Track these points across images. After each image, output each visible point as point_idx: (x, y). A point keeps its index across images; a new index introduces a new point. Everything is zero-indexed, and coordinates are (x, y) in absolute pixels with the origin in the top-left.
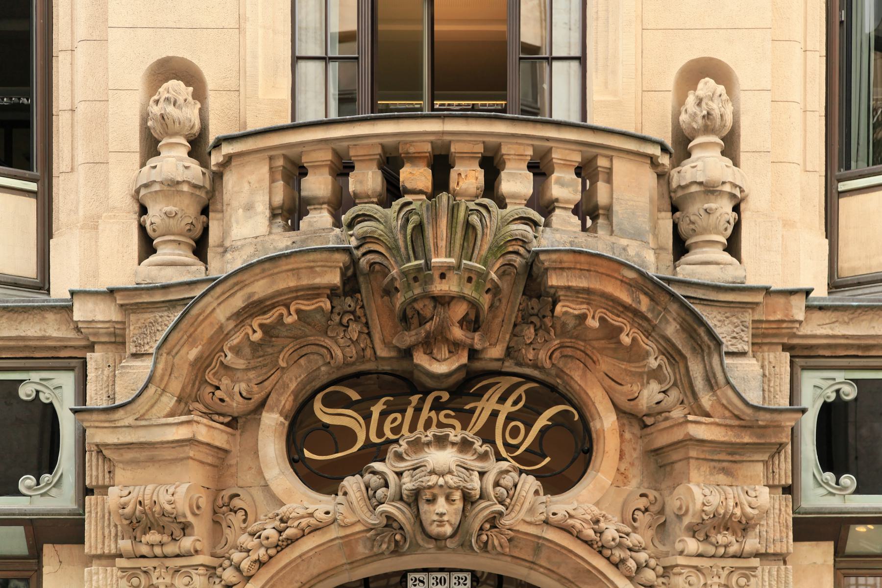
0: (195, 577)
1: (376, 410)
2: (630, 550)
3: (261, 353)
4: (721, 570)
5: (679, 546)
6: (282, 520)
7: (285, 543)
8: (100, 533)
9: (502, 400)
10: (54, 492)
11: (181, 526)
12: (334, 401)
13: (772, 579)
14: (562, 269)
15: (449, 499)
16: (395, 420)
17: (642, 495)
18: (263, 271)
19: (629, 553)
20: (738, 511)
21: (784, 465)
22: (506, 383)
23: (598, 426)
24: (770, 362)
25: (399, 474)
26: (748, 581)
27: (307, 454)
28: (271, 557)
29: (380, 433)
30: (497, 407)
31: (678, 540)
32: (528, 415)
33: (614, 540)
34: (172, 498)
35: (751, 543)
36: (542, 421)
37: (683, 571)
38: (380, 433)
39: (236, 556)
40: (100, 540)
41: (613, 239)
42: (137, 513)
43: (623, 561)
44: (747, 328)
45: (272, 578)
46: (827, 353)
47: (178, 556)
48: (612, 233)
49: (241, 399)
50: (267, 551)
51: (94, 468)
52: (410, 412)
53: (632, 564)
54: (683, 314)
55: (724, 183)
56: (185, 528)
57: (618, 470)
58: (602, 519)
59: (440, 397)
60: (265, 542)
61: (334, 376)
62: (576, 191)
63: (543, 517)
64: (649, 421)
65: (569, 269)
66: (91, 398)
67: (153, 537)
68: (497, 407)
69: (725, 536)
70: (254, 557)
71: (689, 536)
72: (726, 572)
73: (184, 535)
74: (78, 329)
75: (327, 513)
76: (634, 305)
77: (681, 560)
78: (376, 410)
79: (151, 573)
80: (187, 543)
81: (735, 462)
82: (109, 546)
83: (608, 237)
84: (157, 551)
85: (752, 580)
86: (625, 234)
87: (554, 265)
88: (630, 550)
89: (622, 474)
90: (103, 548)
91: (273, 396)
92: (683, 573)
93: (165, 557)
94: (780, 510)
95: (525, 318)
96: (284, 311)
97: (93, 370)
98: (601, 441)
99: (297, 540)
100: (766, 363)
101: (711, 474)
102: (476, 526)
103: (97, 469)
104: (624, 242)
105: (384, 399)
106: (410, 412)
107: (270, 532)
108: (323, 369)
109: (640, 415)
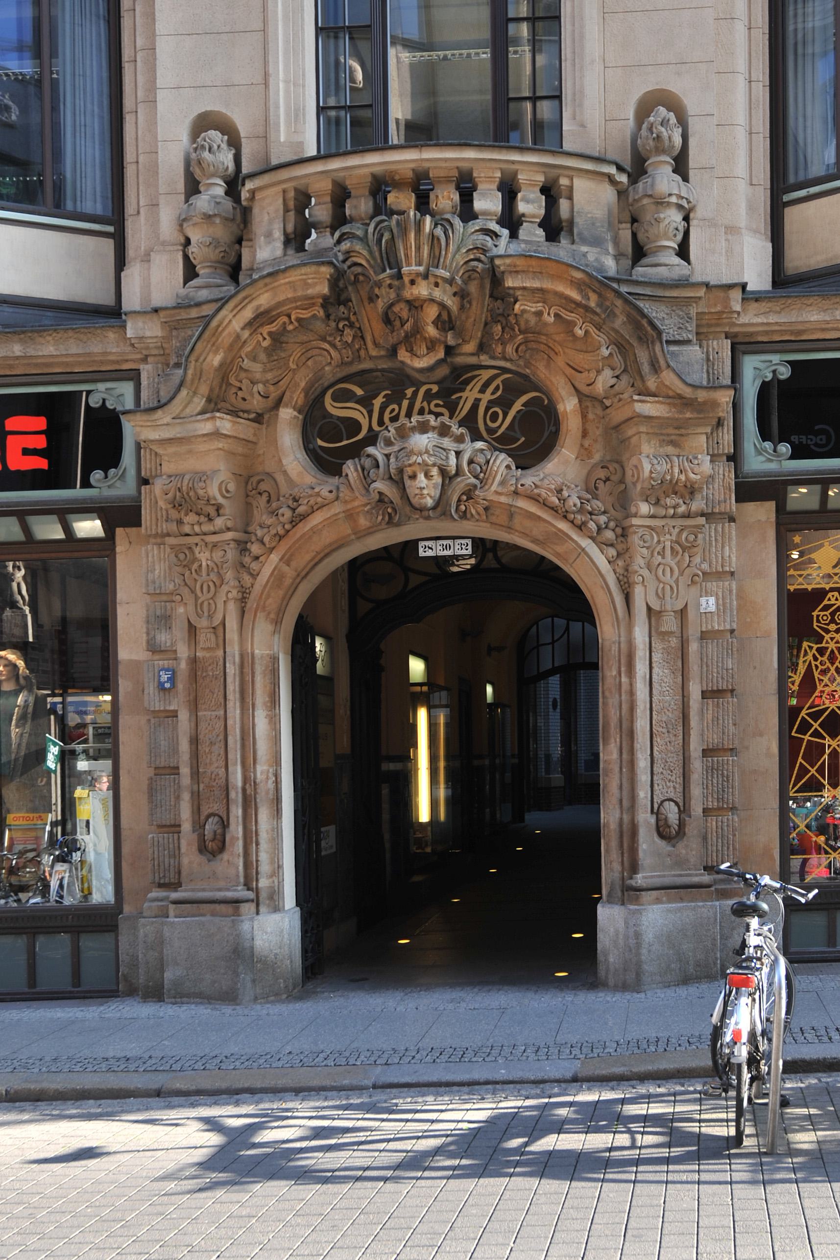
0: (229, 552)
1: (378, 402)
2: (591, 514)
3: (276, 358)
4: (671, 529)
7: (298, 519)
9: (482, 391)
10: (118, 484)
11: (215, 507)
12: (343, 396)
14: (517, 272)
15: (427, 476)
16: (393, 410)
18: (266, 285)
20: (683, 477)
21: (727, 436)
22: (486, 375)
24: (713, 349)
25: (388, 456)
27: (320, 442)
28: (288, 531)
29: (381, 423)
30: (479, 396)
33: (575, 505)
35: (697, 505)
36: (518, 406)
38: (381, 423)
40: (154, 522)
41: (574, 247)
43: (584, 523)
44: (690, 318)
45: (290, 548)
46: (765, 339)
47: (214, 533)
48: (573, 243)
51: (148, 462)
52: (405, 403)
53: (592, 525)
54: (628, 309)
55: (670, 195)
57: (582, 445)
58: (565, 488)
59: (431, 390)
60: (281, 519)
61: (339, 375)
62: (540, 207)
63: (513, 489)
64: (607, 403)
65: (523, 271)
66: (144, 403)
68: (479, 396)
72: (677, 530)
73: (219, 515)
74: (133, 345)
76: (583, 302)
78: (378, 402)
81: (682, 435)
82: (162, 526)
83: (569, 246)
84: (197, 529)
85: (700, 536)
86: (584, 241)
87: (509, 269)
88: (591, 514)
89: (586, 449)
91: (288, 394)
93: (205, 534)
95: (495, 317)
96: (285, 319)
98: (565, 422)
100: (711, 349)
101: (661, 446)
102: (455, 498)
103: (151, 462)
104: (584, 249)
105: (383, 394)
106: (405, 403)
108: (327, 368)
109: (600, 398)
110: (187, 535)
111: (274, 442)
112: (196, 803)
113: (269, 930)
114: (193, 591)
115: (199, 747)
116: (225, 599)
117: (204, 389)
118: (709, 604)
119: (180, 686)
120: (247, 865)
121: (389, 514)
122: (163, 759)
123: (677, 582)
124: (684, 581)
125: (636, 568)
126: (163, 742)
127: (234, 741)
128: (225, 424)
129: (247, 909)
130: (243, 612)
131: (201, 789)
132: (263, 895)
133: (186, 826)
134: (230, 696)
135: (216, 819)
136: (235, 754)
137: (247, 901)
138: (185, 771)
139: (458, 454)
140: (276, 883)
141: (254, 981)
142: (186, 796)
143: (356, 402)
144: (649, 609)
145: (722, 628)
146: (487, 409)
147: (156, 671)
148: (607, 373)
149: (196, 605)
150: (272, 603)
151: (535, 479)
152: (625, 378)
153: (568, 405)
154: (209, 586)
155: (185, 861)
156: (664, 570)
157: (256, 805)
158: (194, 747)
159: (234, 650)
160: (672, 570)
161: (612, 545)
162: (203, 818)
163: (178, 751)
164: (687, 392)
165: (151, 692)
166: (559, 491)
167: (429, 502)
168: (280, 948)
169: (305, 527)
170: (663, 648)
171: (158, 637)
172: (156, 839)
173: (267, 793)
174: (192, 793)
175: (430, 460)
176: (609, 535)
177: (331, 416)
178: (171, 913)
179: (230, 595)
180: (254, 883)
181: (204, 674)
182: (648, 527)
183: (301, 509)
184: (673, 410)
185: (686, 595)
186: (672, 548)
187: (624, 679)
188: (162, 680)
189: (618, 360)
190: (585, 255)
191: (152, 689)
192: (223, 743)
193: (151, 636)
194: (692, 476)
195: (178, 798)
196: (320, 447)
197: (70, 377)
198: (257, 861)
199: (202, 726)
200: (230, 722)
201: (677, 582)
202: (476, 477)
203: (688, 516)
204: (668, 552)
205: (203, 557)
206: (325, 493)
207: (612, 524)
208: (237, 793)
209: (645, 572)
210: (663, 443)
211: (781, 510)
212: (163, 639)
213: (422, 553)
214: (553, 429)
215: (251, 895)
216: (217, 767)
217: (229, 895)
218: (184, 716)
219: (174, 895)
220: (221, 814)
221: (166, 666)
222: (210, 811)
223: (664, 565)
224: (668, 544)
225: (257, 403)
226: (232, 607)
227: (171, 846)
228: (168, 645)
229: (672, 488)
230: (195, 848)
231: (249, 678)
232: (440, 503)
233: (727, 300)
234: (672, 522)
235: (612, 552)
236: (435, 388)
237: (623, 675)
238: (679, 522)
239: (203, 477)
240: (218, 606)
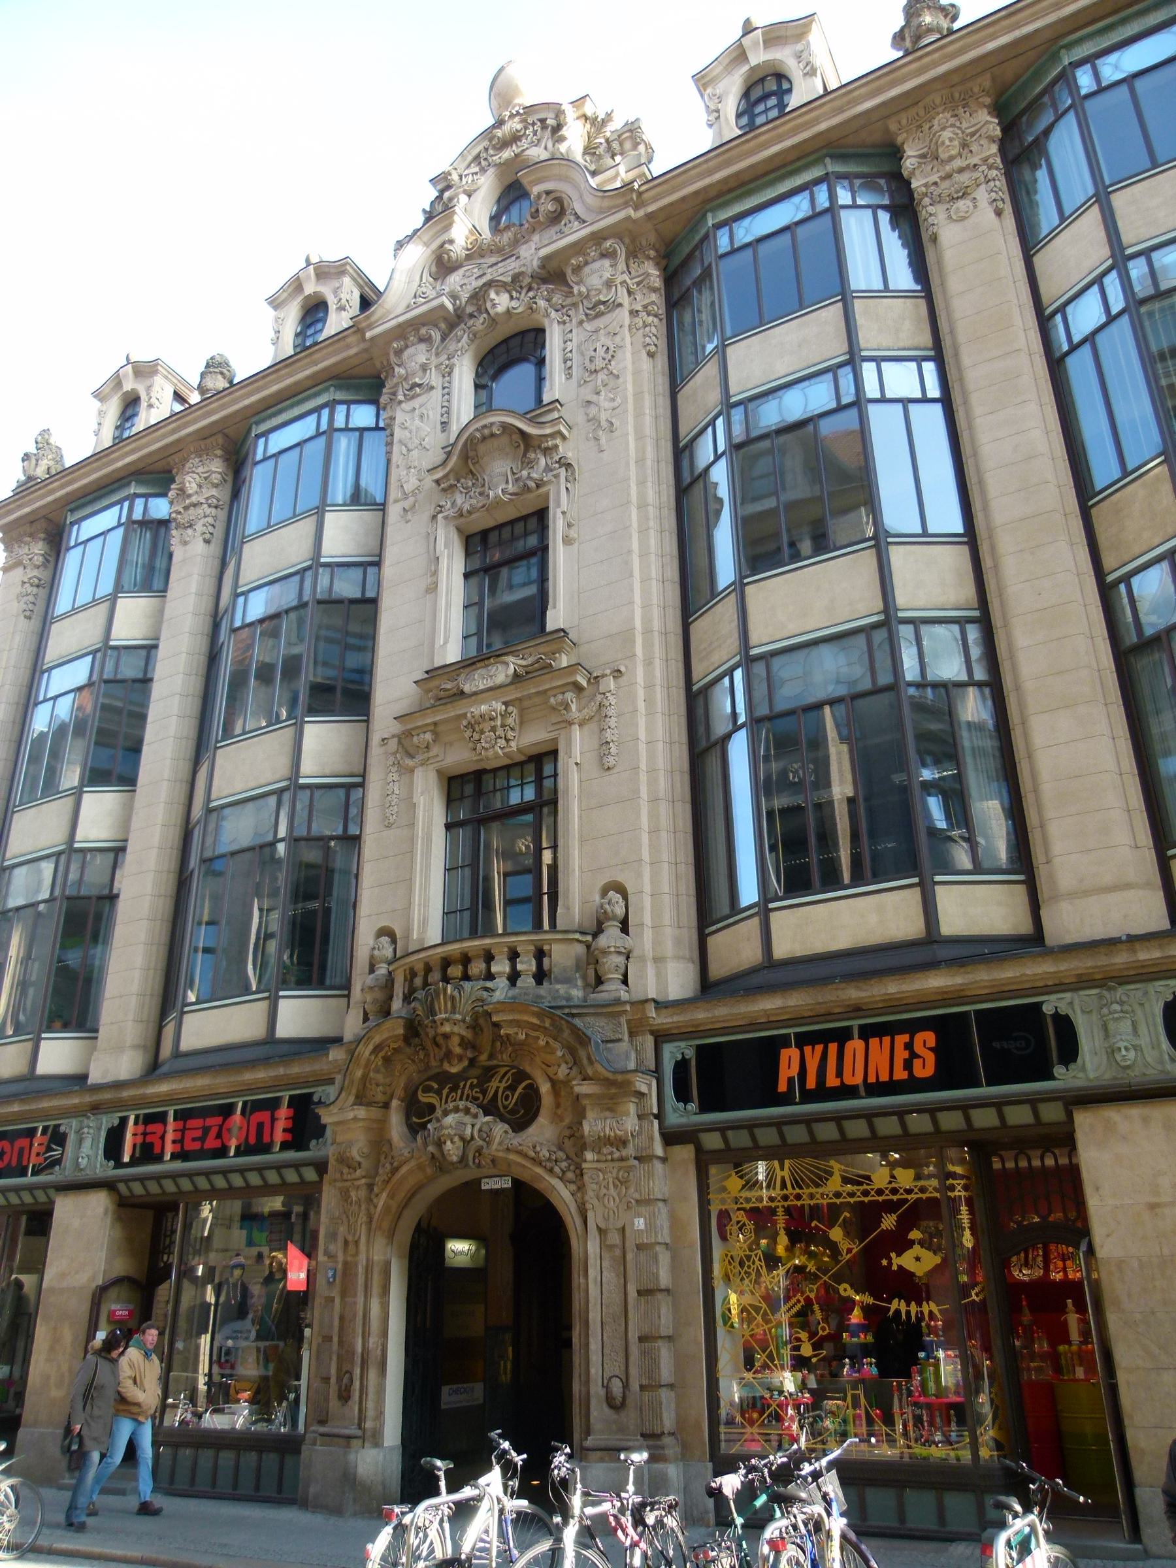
1: (445, 1092)
9: (500, 1081)
12: (428, 1089)
27: (415, 1120)
32: (512, 1088)
36: (520, 1090)
52: (459, 1091)
53: (557, 1169)
78: (445, 1092)
86: (558, 981)
104: (558, 986)
106: (459, 1091)
117: (354, 1091)
120: (360, 1410)
128: (361, 1112)
129: (356, 1443)
132: (368, 1434)
133: (333, 1380)
137: (356, 1437)
138: (335, 1339)
141: (355, 1500)
142: (335, 1358)
148: (564, 1066)
150: (386, 1225)
152: (575, 1069)
153: (545, 1088)
155: (331, 1404)
159: (362, 1258)
161: (573, 1182)
164: (610, 1076)
167: (455, 1159)
169: (398, 1176)
175: (452, 1132)
176: (570, 1175)
177: (419, 1102)
178: (318, 1442)
183: (395, 1164)
189: (569, 1058)
190: (557, 991)
195: (331, 1359)
197: (306, 1084)
202: (484, 1140)
203: (622, 1159)
204: (611, 1186)
205: (353, 1194)
206: (406, 1154)
207: (572, 1168)
209: (595, 1202)
210: (602, 1110)
211: (699, 1150)
213: (483, 1188)
215: (359, 1432)
217: (347, 1432)
218: (338, 1301)
219: (322, 1429)
224: (611, 1180)
225: (380, 1098)
229: (608, 1141)
232: (463, 1159)
233: (644, 1009)
234: (611, 1165)
235: (573, 1187)
236: (475, 1081)
238: (617, 1164)
239: (350, 1144)
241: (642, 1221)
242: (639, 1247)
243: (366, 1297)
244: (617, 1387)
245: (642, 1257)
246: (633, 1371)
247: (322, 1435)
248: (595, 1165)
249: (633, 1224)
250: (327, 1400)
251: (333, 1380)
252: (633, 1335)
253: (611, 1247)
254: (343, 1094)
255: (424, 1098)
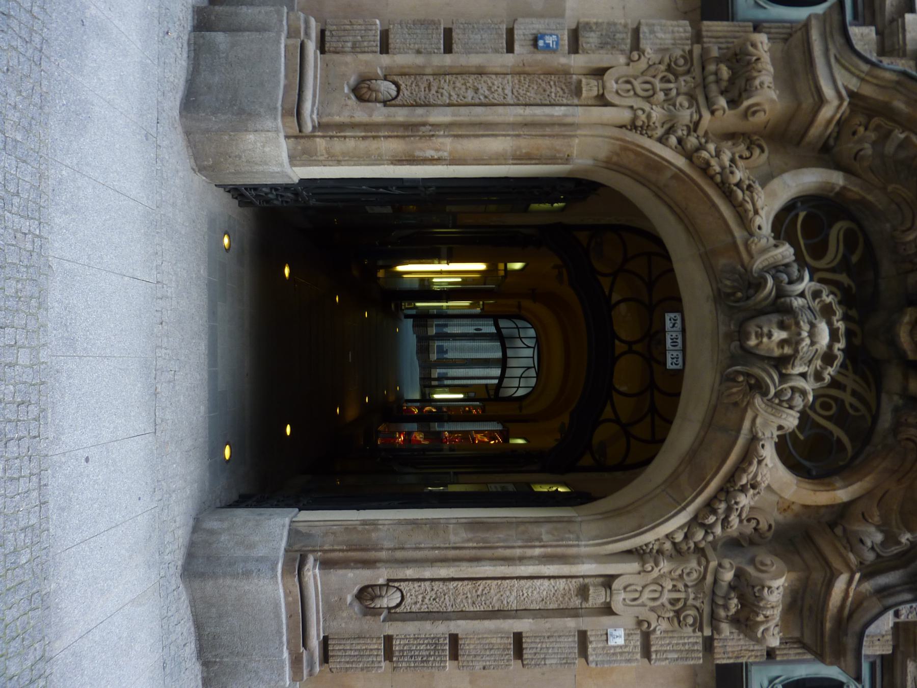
0: (688, 112)
5: (726, 563)
6: (749, 187)
8: (720, 34)
9: (854, 393)
13: (690, 645)
17: (770, 526)
19: (722, 517)
20: (761, 618)
23: (838, 485)
26: (691, 625)
27: (802, 215)
28: (712, 178)
30: (849, 390)
31: (732, 562)
32: (841, 418)
34: (766, 86)
36: (837, 432)
37: (702, 567)
39: (711, 147)
40: (715, 34)
42: (748, 57)
43: (714, 512)
47: (707, 98)
49: (855, 151)
50: (718, 173)
53: (712, 519)
56: (733, 103)
60: (728, 171)
64: (839, 531)
67: (725, 72)
68: (849, 390)
69: (736, 605)
70: (713, 162)
71: (735, 572)
75: (760, 228)
77: (713, 564)
78: (843, 278)
79: (689, 75)
80: (722, 102)
84: (712, 78)
90: (708, 37)
92: (701, 567)
94: (753, 651)
97: (861, 31)
99: (731, 202)
103: (777, 33)
107: (738, 175)
108: (888, 226)
110: (703, 68)
111: (802, 164)
112: (412, 71)
113: (267, 149)
114: (643, 73)
115: (473, 77)
116: (635, 107)
118: (618, 638)
119: (540, 57)
120: (341, 127)
121: (734, 294)
122: (461, 36)
123: (643, 605)
124: (644, 613)
125: (662, 565)
126: (478, 37)
127: (480, 114)
130: (621, 127)
131: (427, 77)
134: (529, 111)
135: (394, 93)
136: (464, 115)
139: (803, 375)
140: (322, 158)
142: (420, 60)
143: (844, 256)
144: (613, 577)
145: (590, 650)
146: (835, 399)
147: (556, 32)
149: (627, 76)
151: (768, 461)
154: (647, 90)
156: (655, 591)
157: (408, 136)
158: (473, 70)
160: (654, 599)
161: (686, 537)
162: (396, 78)
163: (470, 53)
165: (534, 26)
166: (754, 487)
168: (248, 161)
170: (570, 590)
171: (592, 34)
172: (374, 27)
173: (421, 149)
174: (424, 67)
177: (830, 226)
178: (291, 41)
179: (640, 112)
180: (320, 134)
181: (552, 83)
182: (704, 578)
184: (835, 610)
185: (627, 615)
186: (678, 600)
187: (537, 551)
188: (547, 37)
191: (537, 26)
192: (477, 101)
193: (594, 28)
194: (762, 629)
195: (418, 52)
196: (797, 215)
198: (345, 137)
199: (497, 81)
200: (500, 109)
201: (643, 605)
208: (422, 116)
209: (655, 574)
212: (591, 40)
214: (814, 473)
216: (450, 95)
220: (399, 98)
221: (561, 42)
222: (403, 87)
223: (661, 592)
224: (682, 595)
226: (625, 116)
227: (366, 44)
228: (584, 45)
230: (362, 69)
231: (548, 131)
235: (679, 537)
237: (542, 550)
238: (706, 609)
240: (627, 100)
241: (621, 641)
242: (583, 638)
243: (513, 125)
244: (391, 599)
245: (572, 643)
246: (411, 628)
247: (302, 47)
248: (709, 579)
249: (616, 627)
250: (356, 49)
251: (385, 60)
252: (460, 627)
253: (583, 592)
254: (865, 67)
255: (837, 232)
